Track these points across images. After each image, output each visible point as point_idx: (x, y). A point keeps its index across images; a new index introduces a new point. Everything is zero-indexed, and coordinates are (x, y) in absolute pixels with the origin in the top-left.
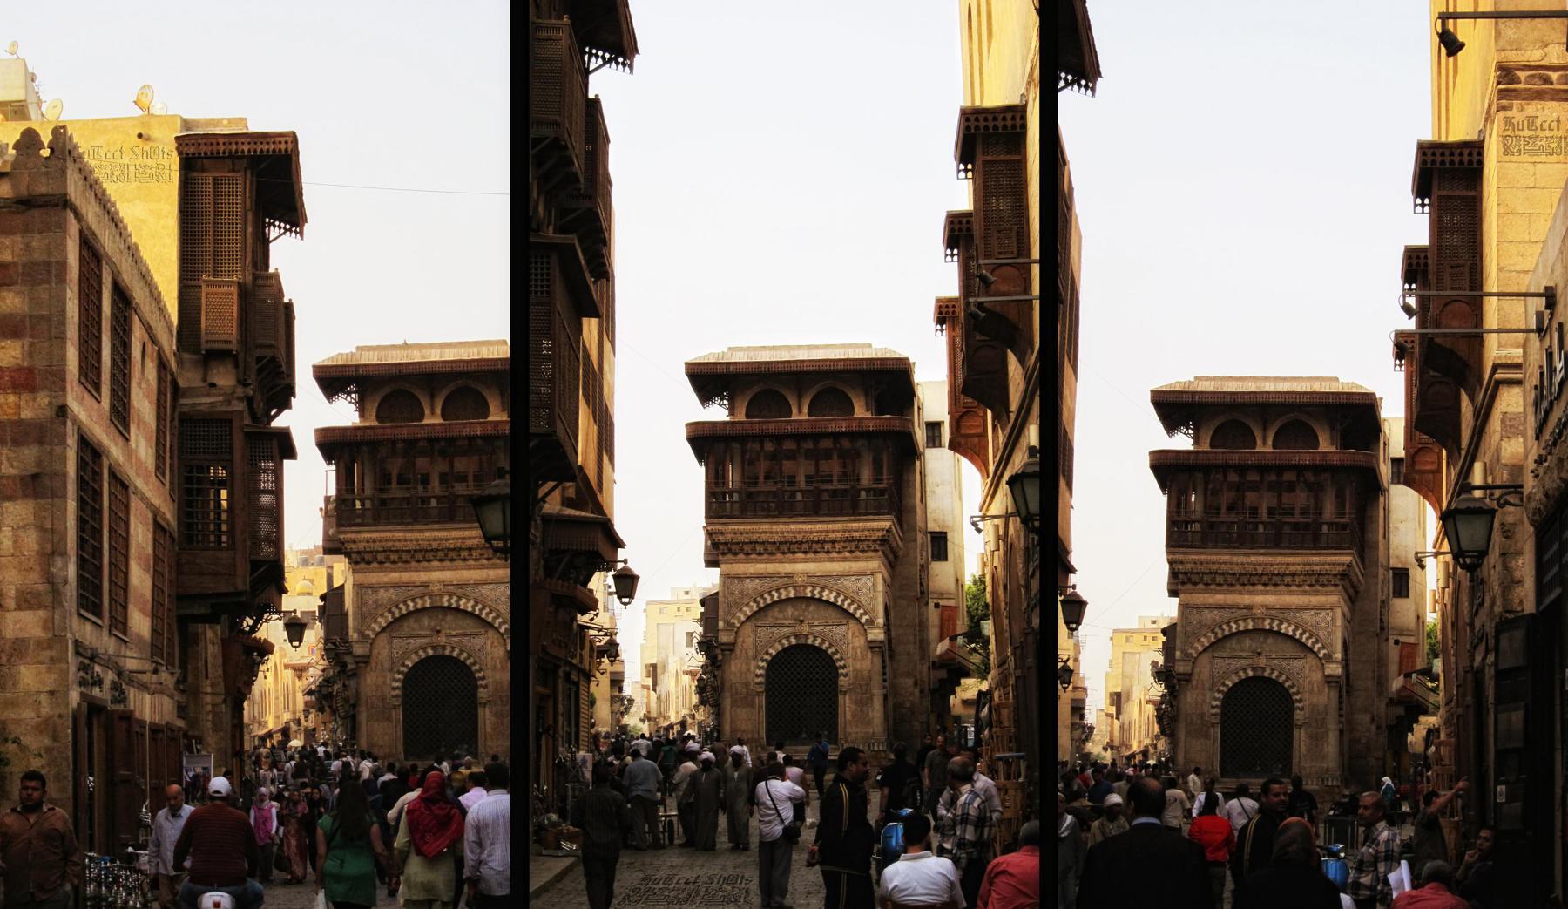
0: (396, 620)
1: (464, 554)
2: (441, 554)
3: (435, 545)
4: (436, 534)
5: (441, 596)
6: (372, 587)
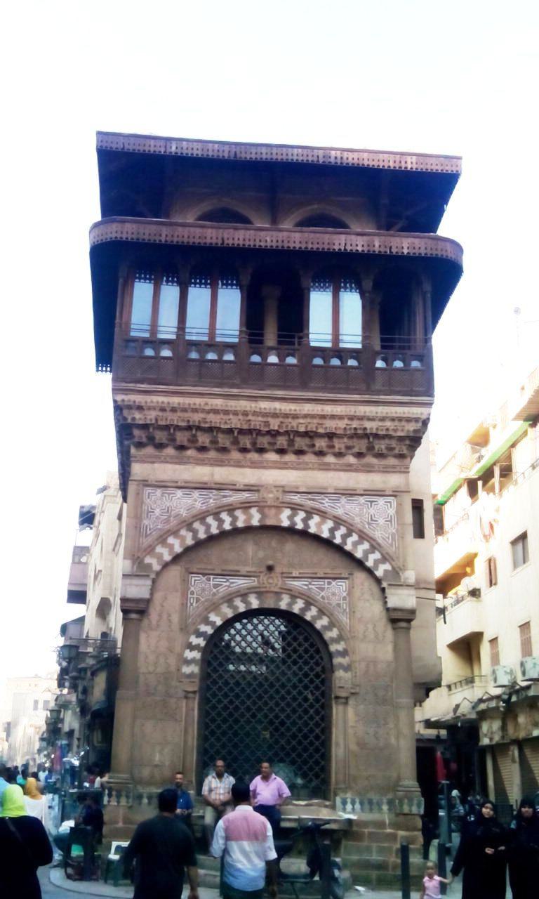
0: (199, 544)
1: (321, 444)
2: (282, 441)
3: (274, 424)
4: (277, 405)
5: (279, 508)
6: (162, 485)
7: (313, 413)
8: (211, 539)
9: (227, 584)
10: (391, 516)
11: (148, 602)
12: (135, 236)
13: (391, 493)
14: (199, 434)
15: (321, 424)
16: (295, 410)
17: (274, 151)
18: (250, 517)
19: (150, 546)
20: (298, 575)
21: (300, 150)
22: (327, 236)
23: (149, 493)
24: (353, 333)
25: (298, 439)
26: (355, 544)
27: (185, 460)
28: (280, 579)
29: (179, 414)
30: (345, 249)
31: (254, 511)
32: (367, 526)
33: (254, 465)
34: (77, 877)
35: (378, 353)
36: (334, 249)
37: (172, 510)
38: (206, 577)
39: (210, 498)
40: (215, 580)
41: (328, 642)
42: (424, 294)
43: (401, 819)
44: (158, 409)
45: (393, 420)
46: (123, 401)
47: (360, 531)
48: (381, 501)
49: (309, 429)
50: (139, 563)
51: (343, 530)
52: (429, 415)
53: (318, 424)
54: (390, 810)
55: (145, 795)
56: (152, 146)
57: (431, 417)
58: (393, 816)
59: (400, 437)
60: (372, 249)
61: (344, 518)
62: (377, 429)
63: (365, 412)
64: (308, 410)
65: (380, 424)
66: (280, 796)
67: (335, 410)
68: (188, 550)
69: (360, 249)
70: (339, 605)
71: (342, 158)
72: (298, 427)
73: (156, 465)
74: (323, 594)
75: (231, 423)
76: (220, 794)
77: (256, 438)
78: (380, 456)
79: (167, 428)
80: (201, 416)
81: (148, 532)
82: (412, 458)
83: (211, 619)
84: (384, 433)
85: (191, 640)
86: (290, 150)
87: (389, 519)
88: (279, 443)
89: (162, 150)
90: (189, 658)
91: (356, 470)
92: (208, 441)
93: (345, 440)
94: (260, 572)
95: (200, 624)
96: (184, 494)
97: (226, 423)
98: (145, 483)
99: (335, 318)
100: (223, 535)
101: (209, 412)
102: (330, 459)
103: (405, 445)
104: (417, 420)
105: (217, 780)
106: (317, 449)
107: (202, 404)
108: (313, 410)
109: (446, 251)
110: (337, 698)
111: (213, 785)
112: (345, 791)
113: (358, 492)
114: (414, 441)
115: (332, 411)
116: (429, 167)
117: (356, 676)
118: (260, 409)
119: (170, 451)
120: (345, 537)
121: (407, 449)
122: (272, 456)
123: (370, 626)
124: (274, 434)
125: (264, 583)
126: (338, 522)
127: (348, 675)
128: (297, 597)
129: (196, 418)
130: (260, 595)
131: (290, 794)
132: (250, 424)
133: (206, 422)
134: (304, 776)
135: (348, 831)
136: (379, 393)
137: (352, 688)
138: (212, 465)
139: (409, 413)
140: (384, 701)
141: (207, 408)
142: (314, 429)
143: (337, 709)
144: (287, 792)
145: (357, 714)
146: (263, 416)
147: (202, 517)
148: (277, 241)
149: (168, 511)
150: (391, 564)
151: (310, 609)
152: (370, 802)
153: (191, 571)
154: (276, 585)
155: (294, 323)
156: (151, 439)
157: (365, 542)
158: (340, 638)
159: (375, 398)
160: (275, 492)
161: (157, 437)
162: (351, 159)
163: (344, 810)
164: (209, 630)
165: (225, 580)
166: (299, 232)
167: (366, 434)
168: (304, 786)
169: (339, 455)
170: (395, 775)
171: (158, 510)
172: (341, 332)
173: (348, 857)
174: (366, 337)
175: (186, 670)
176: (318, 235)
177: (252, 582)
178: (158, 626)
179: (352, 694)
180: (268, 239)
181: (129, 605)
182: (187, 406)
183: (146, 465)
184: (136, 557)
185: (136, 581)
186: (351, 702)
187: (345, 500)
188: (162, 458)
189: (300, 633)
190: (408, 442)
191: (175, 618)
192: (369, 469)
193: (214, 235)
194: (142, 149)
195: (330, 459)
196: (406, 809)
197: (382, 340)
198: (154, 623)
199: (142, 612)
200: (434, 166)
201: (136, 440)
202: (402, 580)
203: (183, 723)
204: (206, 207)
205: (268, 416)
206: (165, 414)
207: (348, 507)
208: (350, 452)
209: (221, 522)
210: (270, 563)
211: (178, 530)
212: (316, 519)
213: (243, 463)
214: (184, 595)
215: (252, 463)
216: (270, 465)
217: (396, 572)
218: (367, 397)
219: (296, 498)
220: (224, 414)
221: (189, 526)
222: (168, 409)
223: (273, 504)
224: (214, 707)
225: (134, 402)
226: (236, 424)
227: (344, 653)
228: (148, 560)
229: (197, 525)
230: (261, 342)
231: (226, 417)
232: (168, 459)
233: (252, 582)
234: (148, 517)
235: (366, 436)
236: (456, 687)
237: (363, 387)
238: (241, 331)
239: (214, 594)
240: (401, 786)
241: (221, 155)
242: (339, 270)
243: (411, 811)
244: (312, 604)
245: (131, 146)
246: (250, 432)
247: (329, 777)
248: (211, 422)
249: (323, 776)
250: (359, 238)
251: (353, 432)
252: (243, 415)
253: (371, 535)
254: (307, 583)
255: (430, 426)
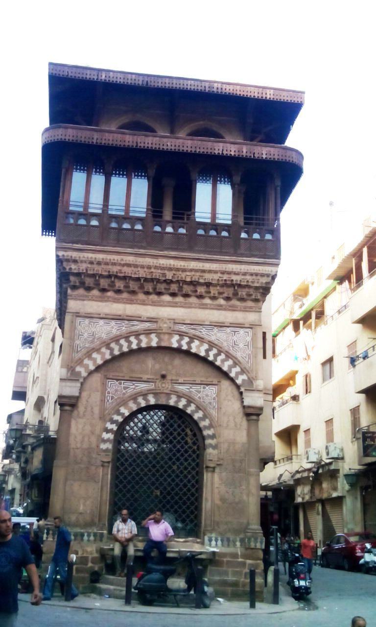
0: (114, 359)
1: (201, 290)
2: (174, 287)
3: (169, 275)
4: (172, 262)
5: (170, 335)
6: (89, 316)
7: (197, 268)
8: (123, 355)
9: (133, 387)
10: (248, 342)
11: (77, 398)
12: (75, 139)
13: (249, 326)
14: (116, 280)
15: (202, 276)
16: (184, 266)
17: (175, 82)
18: (150, 340)
19: (80, 359)
20: (182, 382)
21: (192, 82)
22: (210, 143)
23: (80, 322)
24: (225, 212)
25: (185, 286)
26: (223, 361)
27: (106, 299)
28: (170, 384)
29: (103, 266)
30: (222, 153)
31: (153, 336)
32: (231, 348)
33: (154, 304)
34: (25, 591)
35: (243, 228)
36: (215, 153)
37: (96, 334)
38: (119, 382)
39: (123, 326)
40: (125, 384)
41: (202, 429)
42: (276, 189)
43: (249, 552)
44: (88, 262)
45: (252, 275)
46: (63, 256)
47: (227, 352)
48: (242, 331)
49: (193, 280)
50: (72, 371)
51: (215, 351)
52: (277, 272)
53: (200, 276)
54: (241, 545)
55: (72, 534)
56: (88, 74)
57: (278, 274)
58: (243, 550)
59: (256, 287)
60: (241, 154)
61: (216, 342)
62: (241, 281)
63: (233, 269)
64: (193, 266)
65: (243, 277)
66: (167, 535)
67: (212, 266)
68: (106, 363)
69: (233, 153)
70: (210, 403)
71: (222, 89)
72: (185, 277)
73: (85, 302)
74: (199, 395)
75: (139, 274)
76: (125, 533)
77: (156, 285)
78: (242, 300)
79: (94, 276)
80: (119, 268)
81: (79, 350)
82: (263, 302)
83: (121, 411)
84: (245, 284)
85: (107, 426)
86: (185, 81)
87: (247, 344)
88: (172, 288)
89: (95, 78)
90: (105, 438)
91: (225, 310)
92: (122, 286)
93: (218, 288)
94: (156, 379)
95: (114, 414)
96: (105, 323)
97: (135, 273)
98: (77, 315)
99: (213, 201)
100: (132, 352)
101: (124, 265)
102: (207, 301)
103: (260, 293)
104: (268, 275)
105: (123, 524)
106: (198, 293)
107: (119, 260)
108: (197, 266)
109: (292, 158)
110: (207, 467)
111: (120, 527)
112: (211, 533)
113: (226, 325)
114: (265, 290)
115: (210, 267)
116: (282, 98)
117: (220, 453)
118: (160, 264)
119: (95, 292)
120: (216, 356)
121: (261, 295)
122: (167, 298)
123: (231, 418)
124: (169, 282)
125: (159, 387)
126: (212, 345)
127: (215, 452)
128: (181, 397)
129: (115, 269)
130: (156, 395)
131: (173, 534)
132: (152, 275)
133: (121, 273)
134: (183, 521)
135: (214, 559)
136: (242, 255)
137: (218, 461)
138: (125, 303)
139: (263, 270)
140: (239, 471)
141: (122, 262)
142: (197, 280)
143: (207, 476)
144: (171, 532)
145: (221, 479)
146: (161, 269)
147: (116, 339)
148: (175, 146)
149: (93, 334)
150: (247, 375)
151: (190, 406)
152: (228, 540)
153: (108, 377)
154: (168, 388)
155: (184, 204)
156: (82, 284)
157: (230, 360)
158: (210, 426)
159: (240, 259)
160: (169, 323)
161: (87, 282)
162: (229, 89)
163: (210, 545)
164: (120, 419)
165: (132, 384)
166: (191, 140)
167: (233, 284)
168: (183, 529)
169: (214, 298)
170: (245, 521)
171: (86, 334)
172: (217, 212)
173: (211, 578)
174: (234, 216)
175: (104, 446)
176: (204, 143)
177: (151, 386)
178: (84, 415)
179: (218, 465)
180: (169, 144)
181: (64, 401)
182: (108, 261)
183: (78, 302)
184: (69, 367)
185: (69, 384)
186: (217, 470)
187: (217, 330)
188: (90, 298)
189: (183, 423)
190: (261, 291)
191: (96, 411)
192: (233, 309)
193: (131, 140)
194: (81, 76)
195: (207, 301)
196: (252, 545)
197: (245, 219)
198: (81, 413)
199: (74, 406)
200: (285, 97)
201: (72, 284)
202: (254, 387)
203: (100, 483)
204: (125, 119)
205: (165, 270)
206: (93, 266)
207: (219, 335)
208: (221, 296)
209: (130, 343)
210: (164, 373)
211: (100, 349)
212: (197, 343)
213: (146, 302)
214: (103, 394)
215: (152, 302)
216: (165, 304)
217: (250, 381)
218: (234, 258)
219: (183, 327)
220: (134, 267)
221: (108, 346)
222: (95, 263)
223: (167, 332)
224: (122, 473)
225: (71, 257)
226: (142, 275)
227: (213, 437)
228: (78, 369)
229: (113, 345)
230: (161, 217)
231: (135, 270)
232: (94, 298)
233: (151, 386)
234: (79, 338)
235: (233, 285)
236: (284, 462)
237: (232, 251)
238: (147, 209)
239: (124, 394)
240: (249, 529)
241: (235, 93)
242: (217, 168)
243: (256, 546)
244: (191, 402)
245: (72, 74)
246: (152, 280)
247: (201, 523)
248: (125, 272)
249: (196, 522)
250: (232, 145)
251: (223, 282)
252: (148, 268)
253: (234, 355)
254: (189, 387)
255: (276, 280)
